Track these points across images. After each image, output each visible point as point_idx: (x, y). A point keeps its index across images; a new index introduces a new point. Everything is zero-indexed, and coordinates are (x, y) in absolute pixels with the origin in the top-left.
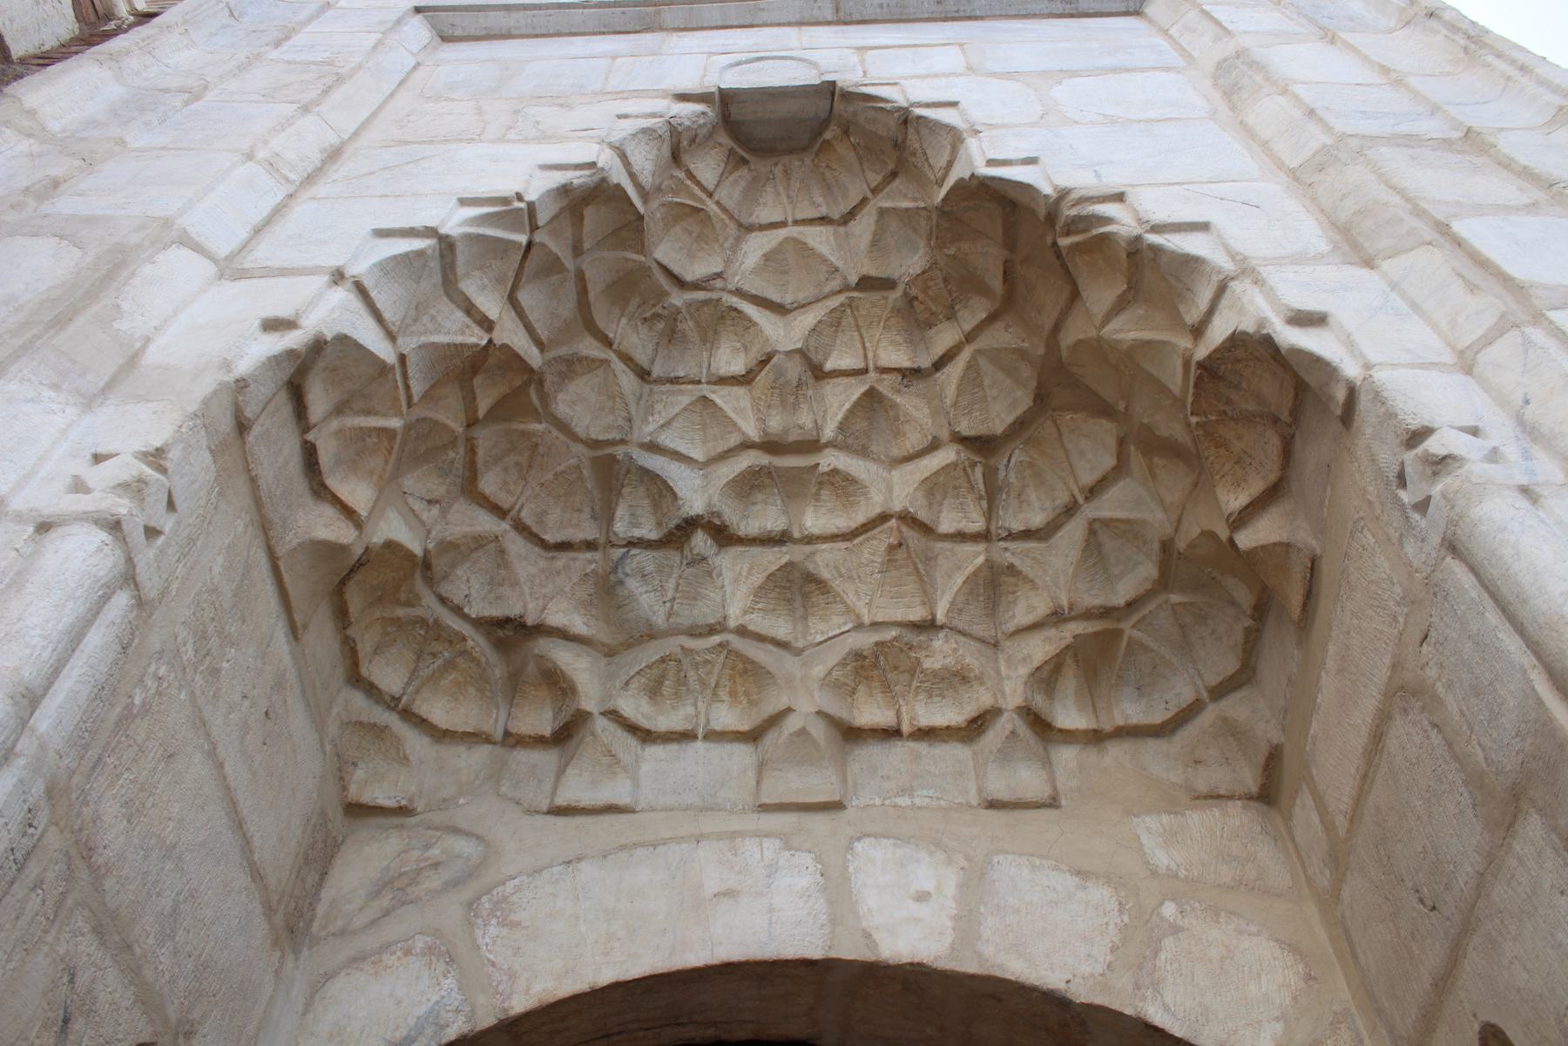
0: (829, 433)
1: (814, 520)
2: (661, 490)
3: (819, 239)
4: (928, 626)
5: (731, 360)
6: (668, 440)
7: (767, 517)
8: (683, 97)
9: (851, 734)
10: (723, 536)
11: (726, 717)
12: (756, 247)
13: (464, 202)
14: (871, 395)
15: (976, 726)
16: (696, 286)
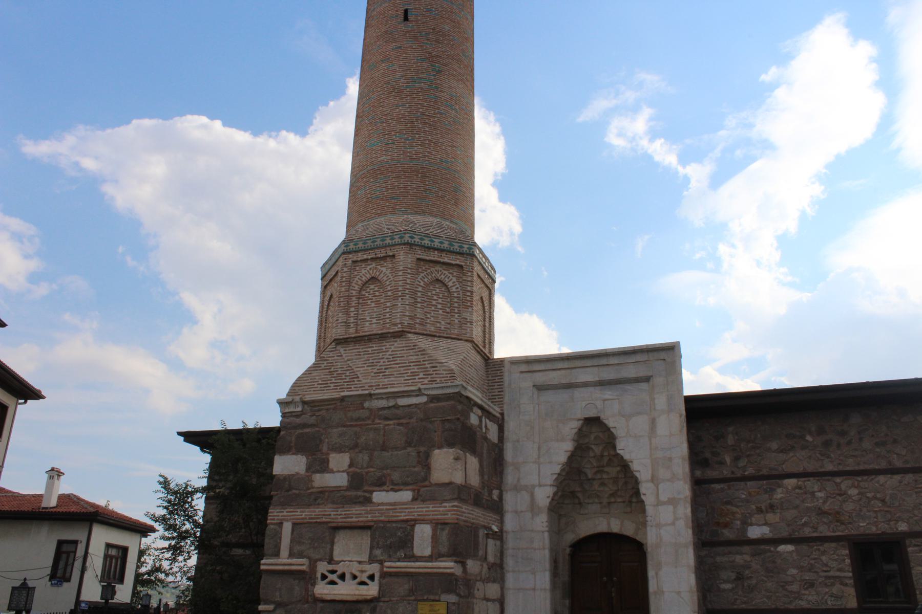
0: (605, 464)
1: (605, 476)
2: (586, 475)
3: (601, 435)
4: (618, 490)
5: (592, 454)
6: (586, 466)
7: (599, 476)
8: (579, 420)
9: (609, 503)
10: (594, 479)
11: (596, 500)
12: (592, 437)
13: (558, 464)
14: (610, 460)
15: (624, 502)
16: (586, 444)
